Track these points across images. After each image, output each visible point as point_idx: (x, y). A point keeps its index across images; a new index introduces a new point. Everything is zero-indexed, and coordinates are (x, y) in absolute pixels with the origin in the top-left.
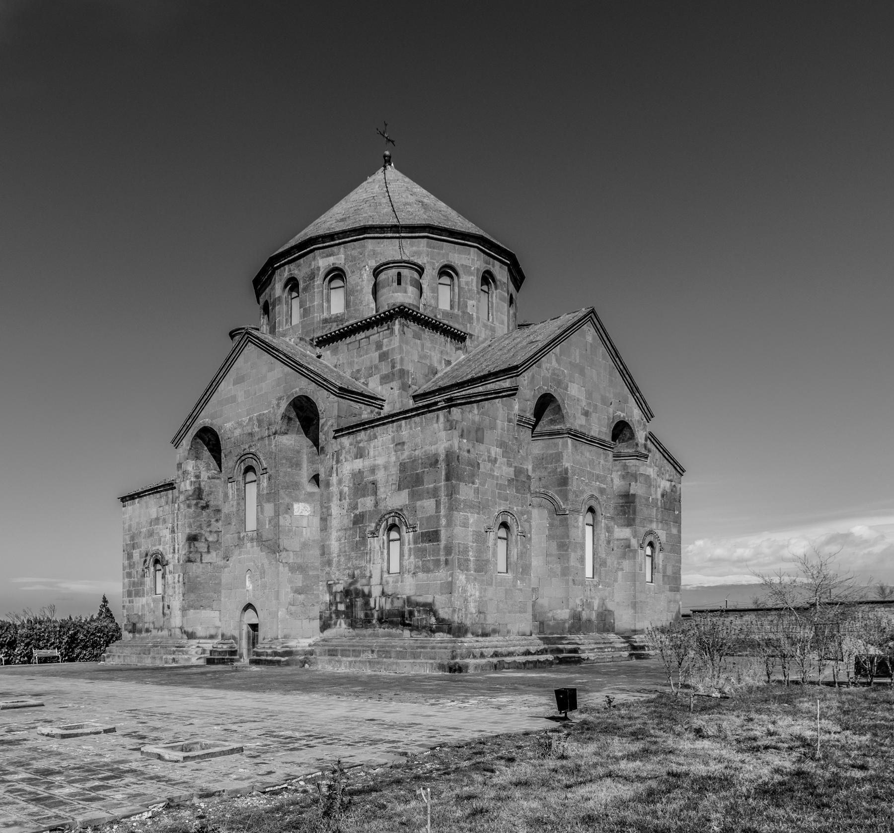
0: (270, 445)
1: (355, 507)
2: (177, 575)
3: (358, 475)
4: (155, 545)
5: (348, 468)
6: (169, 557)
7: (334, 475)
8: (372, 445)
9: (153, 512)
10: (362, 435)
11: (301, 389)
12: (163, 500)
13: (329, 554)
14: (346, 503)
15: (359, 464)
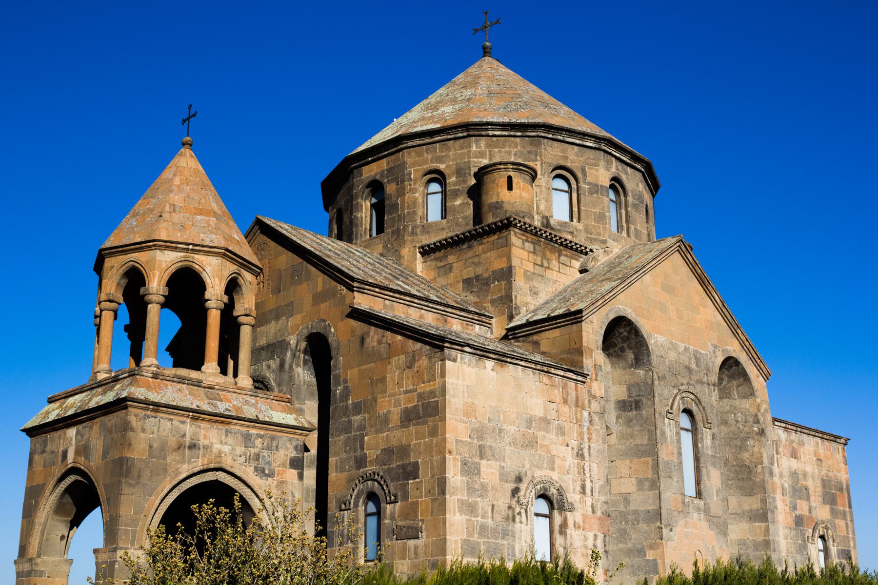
0: (711, 396)
1: (795, 508)
2: (590, 535)
3: (794, 474)
4: (540, 467)
5: (787, 463)
6: (573, 496)
7: (776, 465)
8: (802, 450)
9: (537, 405)
10: (793, 434)
11: (734, 351)
12: (557, 394)
13: (780, 552)
14: (788, 499)
15: (794, 464)
